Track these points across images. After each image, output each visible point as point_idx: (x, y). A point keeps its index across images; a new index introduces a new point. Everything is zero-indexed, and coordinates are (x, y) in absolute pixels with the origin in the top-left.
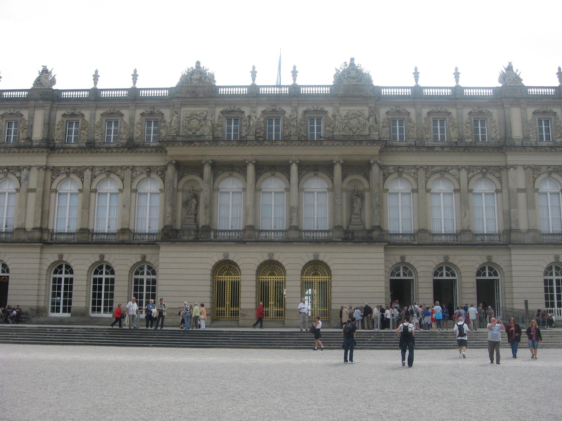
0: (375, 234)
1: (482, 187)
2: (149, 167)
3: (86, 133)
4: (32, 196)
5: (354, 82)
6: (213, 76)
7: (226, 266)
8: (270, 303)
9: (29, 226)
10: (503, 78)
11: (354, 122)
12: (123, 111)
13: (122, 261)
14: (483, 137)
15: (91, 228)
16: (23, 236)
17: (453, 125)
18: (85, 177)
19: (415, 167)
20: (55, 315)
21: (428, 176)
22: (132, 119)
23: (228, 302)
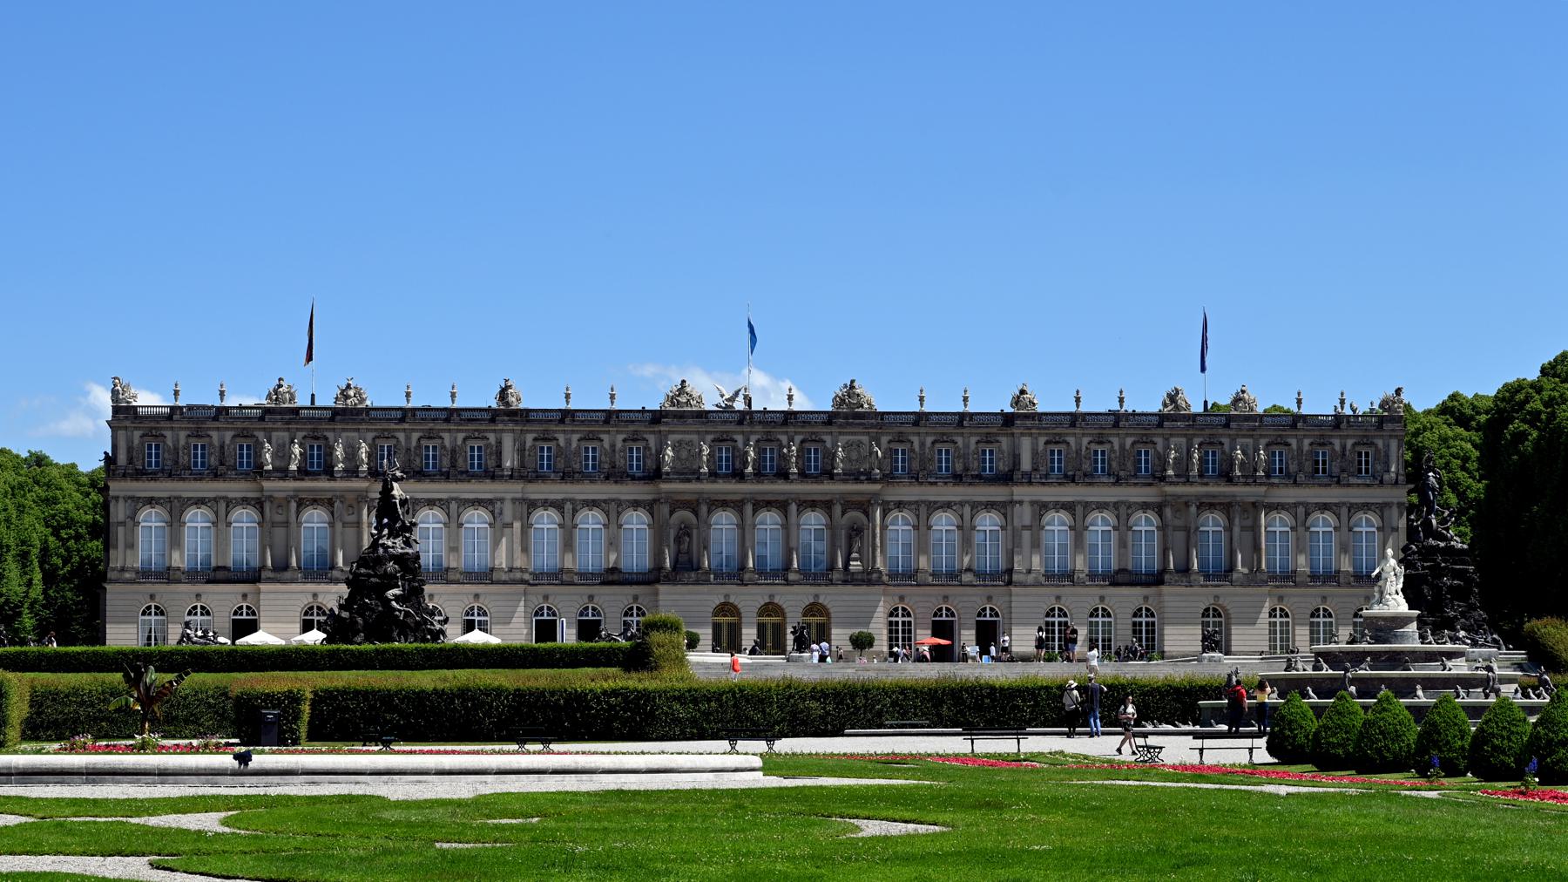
7: (726, 608)
10: (1016, 402)
12: (602, 436)
16: (504, 577)
19: (916, 502)
22: (613, 446)
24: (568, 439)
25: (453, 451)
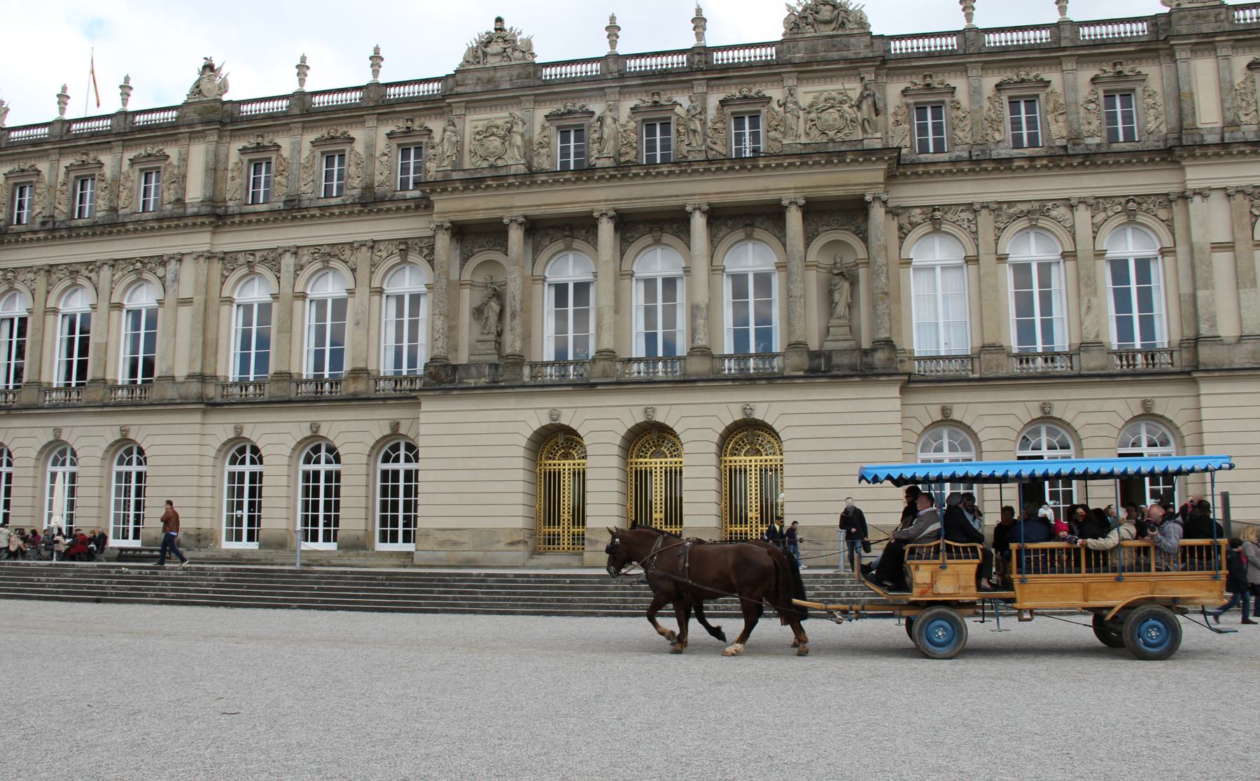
0: (880, 357)
2: (404, 241)
3: (284, 181)
4: (185, 311)
5: (827, 30)
6: (528, 43)
8: (654, 516)
9: (181, 372)
11: (831, 116)
12: (353, 133)
13: (356, 433)
14: (1129, 134)
15: (294, 370)
16: (171, 393)
17: (1055, 110)
18: (283, 268)
19: (969, 207)
20: (234, 545)
21: (1002, 226)
22: (370, 146)
23: (566, 516)
25: (116, 181)
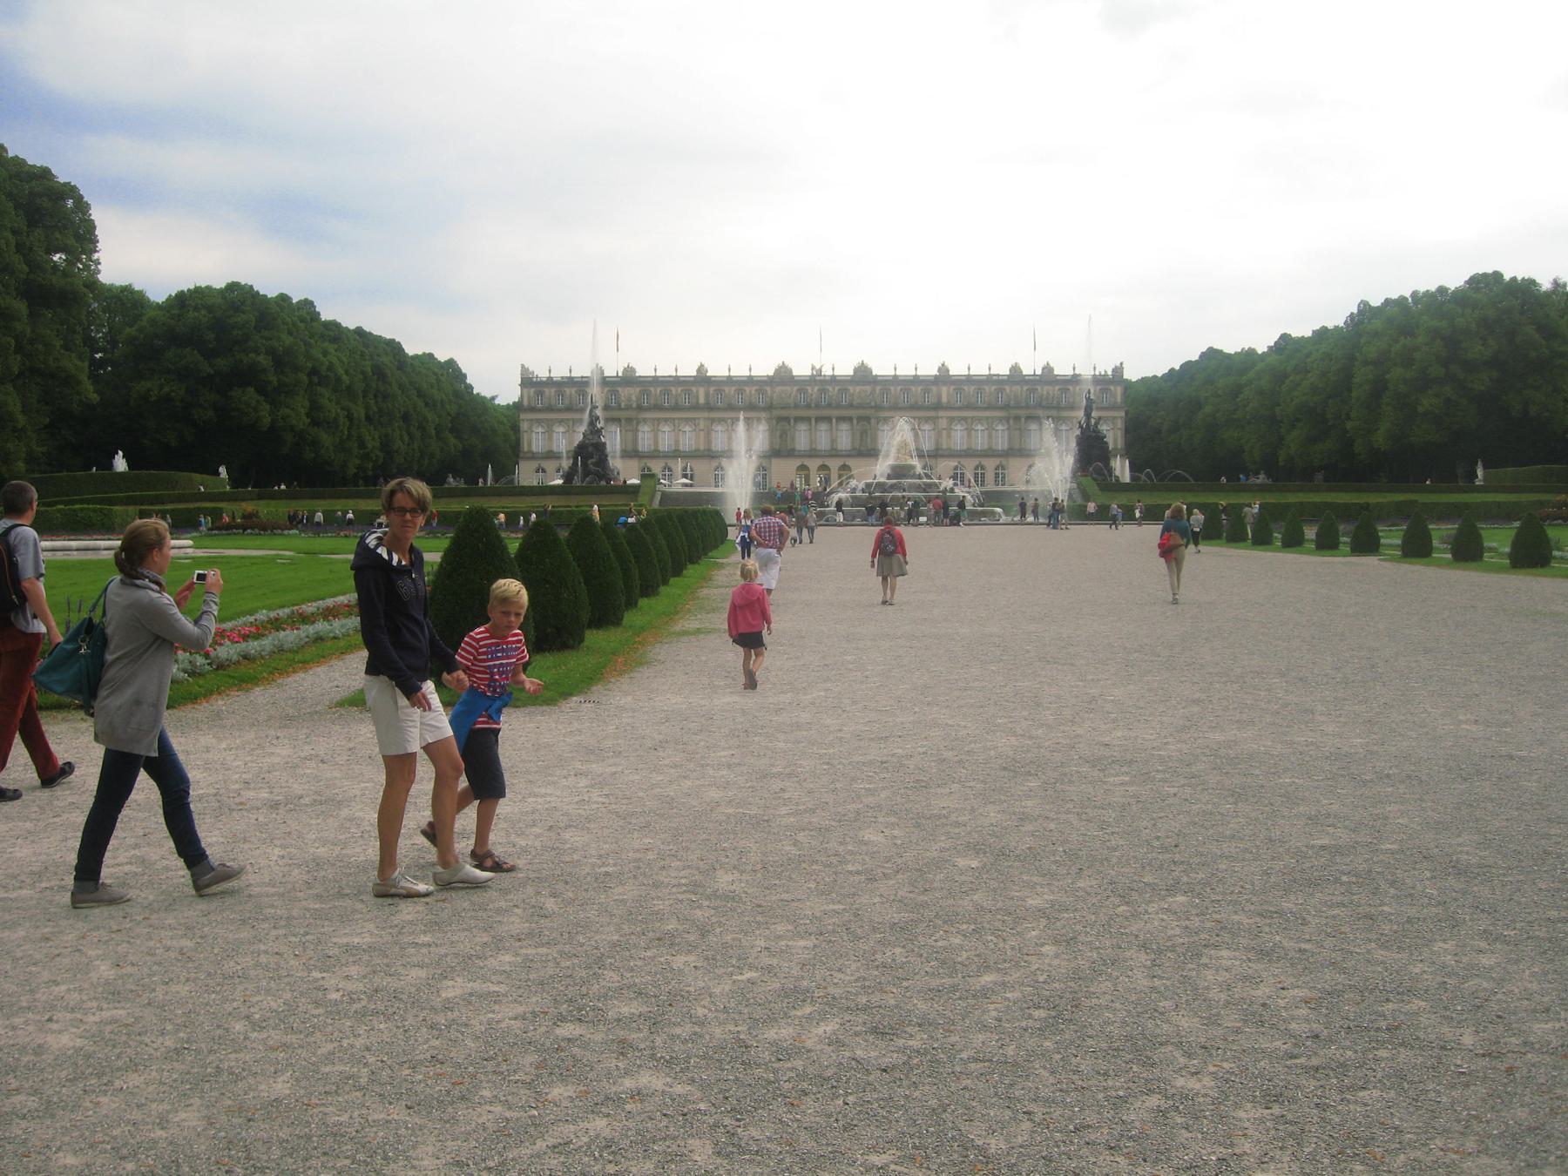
1: (927, 427)
7: (803, 468)
24: (730, 390)
